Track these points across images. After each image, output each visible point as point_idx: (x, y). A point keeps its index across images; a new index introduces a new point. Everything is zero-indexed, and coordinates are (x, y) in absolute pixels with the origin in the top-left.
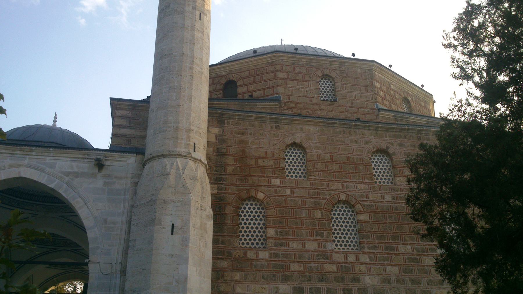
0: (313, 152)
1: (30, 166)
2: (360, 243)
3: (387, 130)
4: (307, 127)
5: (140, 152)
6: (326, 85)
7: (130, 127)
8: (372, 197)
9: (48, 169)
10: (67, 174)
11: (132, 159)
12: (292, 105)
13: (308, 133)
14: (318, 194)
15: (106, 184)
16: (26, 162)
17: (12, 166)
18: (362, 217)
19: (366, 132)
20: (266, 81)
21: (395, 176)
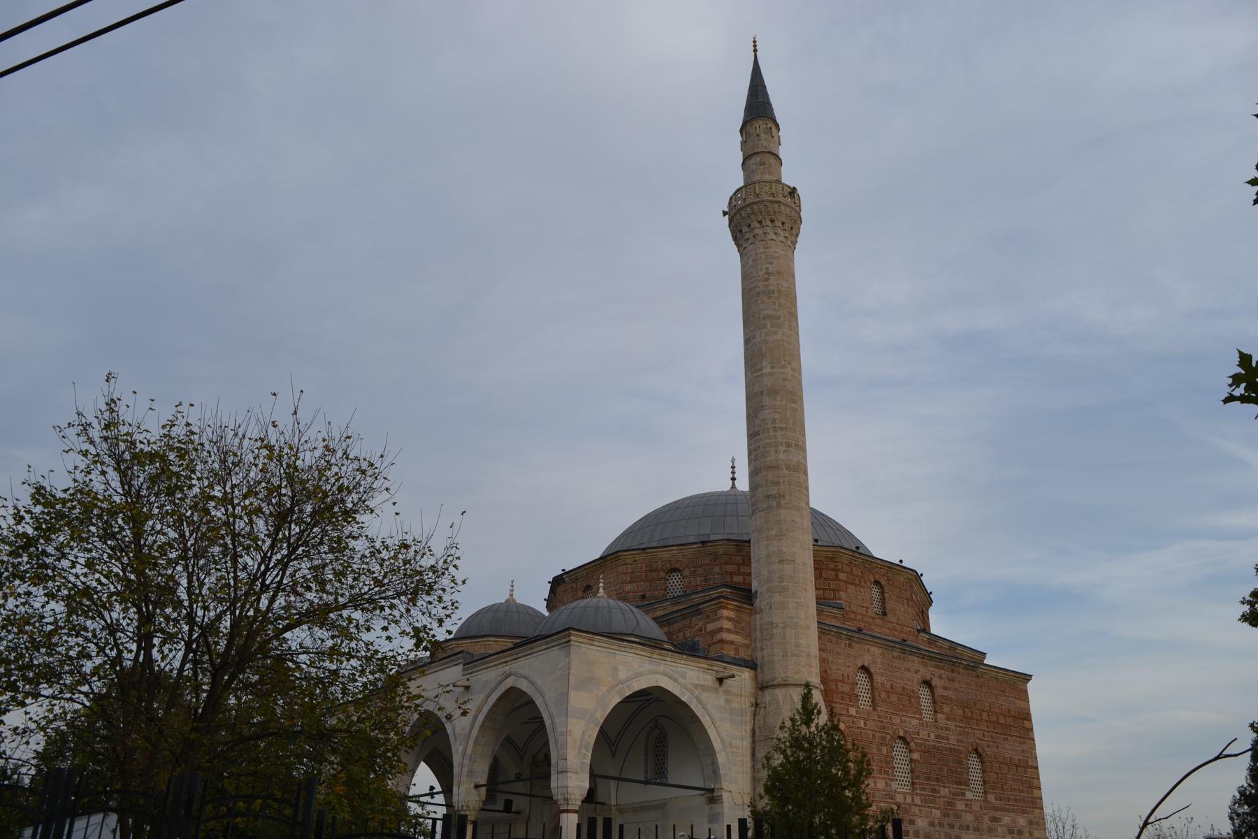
0: (878, 679)
1: (665, 674)
2: (913, 783)
3: (931, 658)
4: (872, 648)
5: (752, 665)
6: (875, 591)
7: (736, 633)
8: (923, 734)
9: (680, 679)
10: (697, 686)
11: (745, 676)
12: (853, 616)
13: (872, 655)
14: (884, 727)
15: (727, 701)
16: (662, 668)
17: (651, 672)
18: (916, 756)
19: (916, 659)
20: (826, 579)
21: (936, 712)
